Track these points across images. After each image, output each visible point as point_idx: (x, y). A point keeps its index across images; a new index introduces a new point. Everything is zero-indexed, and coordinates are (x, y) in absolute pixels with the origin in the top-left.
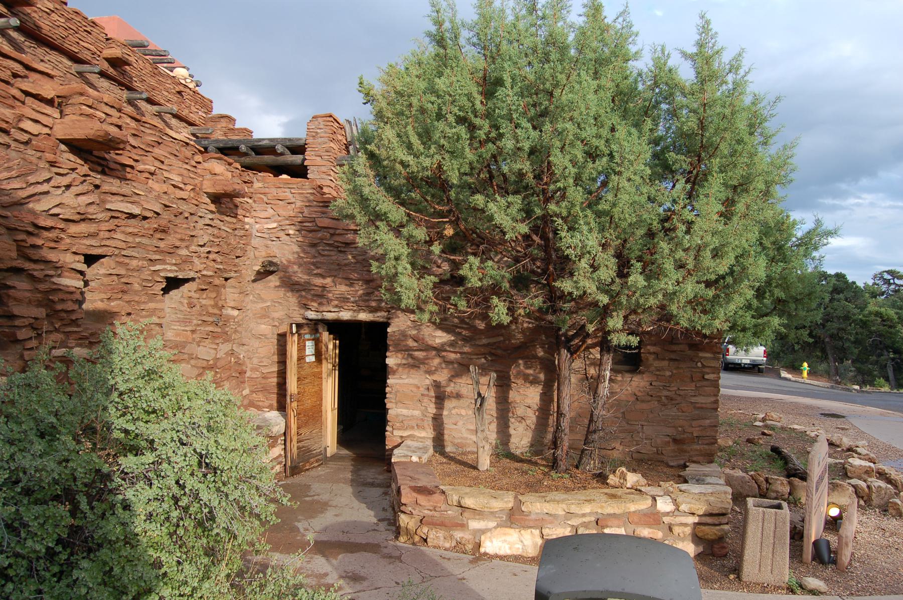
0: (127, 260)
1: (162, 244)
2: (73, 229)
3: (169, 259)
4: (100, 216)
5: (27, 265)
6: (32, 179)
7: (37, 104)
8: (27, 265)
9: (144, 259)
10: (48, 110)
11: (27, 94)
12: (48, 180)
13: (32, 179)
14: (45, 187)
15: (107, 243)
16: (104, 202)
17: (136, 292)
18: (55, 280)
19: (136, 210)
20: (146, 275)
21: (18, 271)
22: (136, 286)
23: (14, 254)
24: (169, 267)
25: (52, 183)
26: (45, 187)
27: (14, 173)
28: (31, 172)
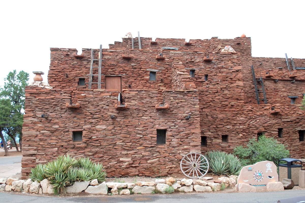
0: (288, 128)
1: (297, 125)
2: (275, 125)
3: (299, 127)
4: (280, 122)
5: (267, 131)
6: (266, 120)
7: (267, 110)
8: (267, 131)
9: (293, 128)
10: (269, 110)
11: (265, 109)
12: (269, 119)
13: (266, 120)
14: (269, 120)
15: (283, 126)
16: (281, 120)
17: (291, 133)
18: (272, 132)
19: (289, 120)
20: (293, 130)
21: (266, 132)
22: (291, 132)
23: (264, 130)
24: (299, 128)
25: (270, 119)
26: (269, 120)
27: (263, 120)
28: (266, 119)
